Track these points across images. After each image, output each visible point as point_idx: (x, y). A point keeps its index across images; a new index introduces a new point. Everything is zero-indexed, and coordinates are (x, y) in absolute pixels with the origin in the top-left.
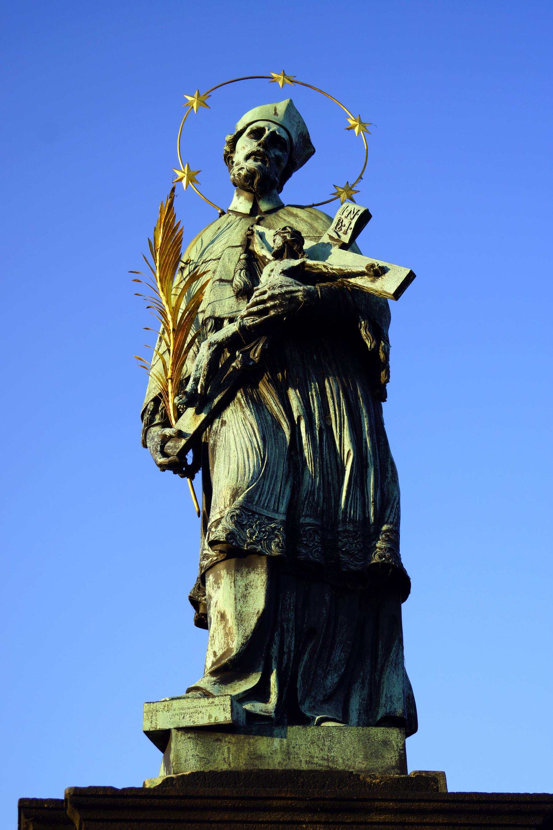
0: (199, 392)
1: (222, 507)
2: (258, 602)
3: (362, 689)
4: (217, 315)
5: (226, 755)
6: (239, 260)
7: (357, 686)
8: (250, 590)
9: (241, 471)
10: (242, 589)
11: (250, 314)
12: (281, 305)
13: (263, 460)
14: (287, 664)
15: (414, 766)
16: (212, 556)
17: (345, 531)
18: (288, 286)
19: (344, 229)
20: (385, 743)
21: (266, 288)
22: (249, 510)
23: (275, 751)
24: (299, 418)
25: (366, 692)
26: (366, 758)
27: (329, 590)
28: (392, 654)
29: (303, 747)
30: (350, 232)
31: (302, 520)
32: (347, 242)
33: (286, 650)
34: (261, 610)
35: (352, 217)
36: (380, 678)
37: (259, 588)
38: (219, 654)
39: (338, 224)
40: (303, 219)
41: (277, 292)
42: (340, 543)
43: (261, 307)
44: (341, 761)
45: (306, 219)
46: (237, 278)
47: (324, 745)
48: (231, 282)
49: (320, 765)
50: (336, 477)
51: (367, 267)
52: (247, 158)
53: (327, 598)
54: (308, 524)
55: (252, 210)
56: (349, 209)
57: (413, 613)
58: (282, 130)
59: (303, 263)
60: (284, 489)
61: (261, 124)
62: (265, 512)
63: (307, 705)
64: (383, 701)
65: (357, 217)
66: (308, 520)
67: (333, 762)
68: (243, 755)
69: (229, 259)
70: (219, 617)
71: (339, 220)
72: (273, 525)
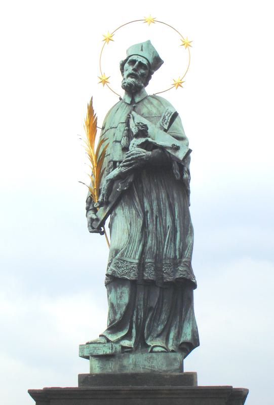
2: (126, 299)
4: (114, 160)
5: (111, 366)
6: (124, 130)
7: (173, 328)
13: (129, 235)
14: (140, 323)
15: (187, 369)
17: (166, 263)
19: (166, 121)
20: (175, 359)
22: (122, 260)
23: (130, 364)
24: (147, 212)
25: (177, 330)
26: (167, 366)
27: (156, 293)
29: (141, 362)
30: (168, 124)
31: (146, 261)
32: (166, 128)
33: (139, 317)
34: (127, 303)
40: (154, 106)
41: (134, 156)
42: (164, 269)
46: (122, 141)
47: (150, 361)
48: (120, 142)
50: (163, 237)
52: (128, 76)
54: (149, 262)
57: (198, 296)
58: (144, 59)
59: (147, 141)
60: (139, 247)
61: (134, 58)
62: (129, 260)
63: (149, 339)
64: (183, 335)
65: (171, 116)
66: (149, 260)
68: (118, 366)
72: (132, 266)
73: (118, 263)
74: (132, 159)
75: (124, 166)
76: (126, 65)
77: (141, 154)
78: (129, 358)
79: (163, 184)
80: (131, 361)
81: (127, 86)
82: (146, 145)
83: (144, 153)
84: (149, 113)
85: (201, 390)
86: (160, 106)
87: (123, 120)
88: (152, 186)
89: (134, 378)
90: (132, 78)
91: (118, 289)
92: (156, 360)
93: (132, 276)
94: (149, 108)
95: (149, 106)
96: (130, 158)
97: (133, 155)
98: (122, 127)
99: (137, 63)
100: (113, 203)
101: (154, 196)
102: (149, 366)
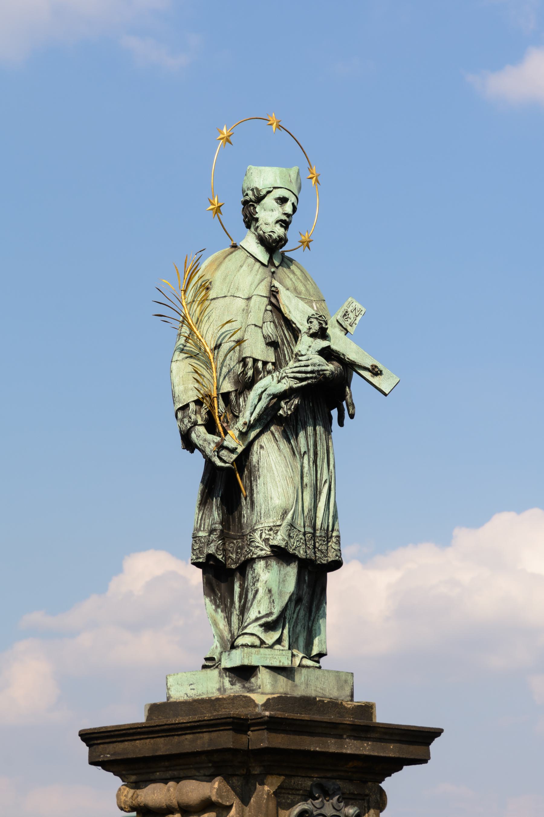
0: (252, 422)
1: (275, 519)
2: (291, 586)
3: (304, 631)
4: (254, 356)
6: (266, 310)
8: (287, 577)
9: (286, 495)
10: (282, 576)
11: (295, 378)
12: (315, 378)
16: (266, 550)
18: (323, 365)
19: (350, 321)
21: (309, 362)
22: (292, 526)
23: (302, 683)
24: (305, 452)
25: (305, 634)
26: (338, 690)
28: (321, 612)
29: (313, 681)
34: (292, 592)
35: (357, 314)
36: (312, 625)
37: (292, 577)
38: (263, 613)
39: (345, 315)
40: (299, 278)
41: (316, 368)
43: (304, 375)
44: (328, 690)
45: (301, 278)
48: (261, 328)
49: (320, 693)
51: (372, 366)
52: (277, 222)
53: (307, 578)
54: (309, 533)
55: (269, 262)
56: (354, 305)
67: (325, 690)
69: (259, 307)
70: (267, 590)
71: (347, 312)
73: (290, 530)
74: (312, 372)
75: (295, 378)
76: (269, 201)
77: (323, 368)
78: (301, 673)
79: (320, 410)
80: (303, 679)
81: (276, 239)
82: (328, 354)
83: (330, 367)
84: (295, 289)
85: (392, 728)
86: (306, 281)
87: (263, 290)
88: (308, 412)
89: (307, 702)
90: (281, 226)
91: (282, 569)
92: (327, 680)
93: (301, 553)
94: (294, 280)
95: (292, 276)
96: (309, 369)
97: (314, 365)
98: (260, 304)
99: (289, 204)
100: (258, 430)
101: (310, 429)
102: (321, 689)
